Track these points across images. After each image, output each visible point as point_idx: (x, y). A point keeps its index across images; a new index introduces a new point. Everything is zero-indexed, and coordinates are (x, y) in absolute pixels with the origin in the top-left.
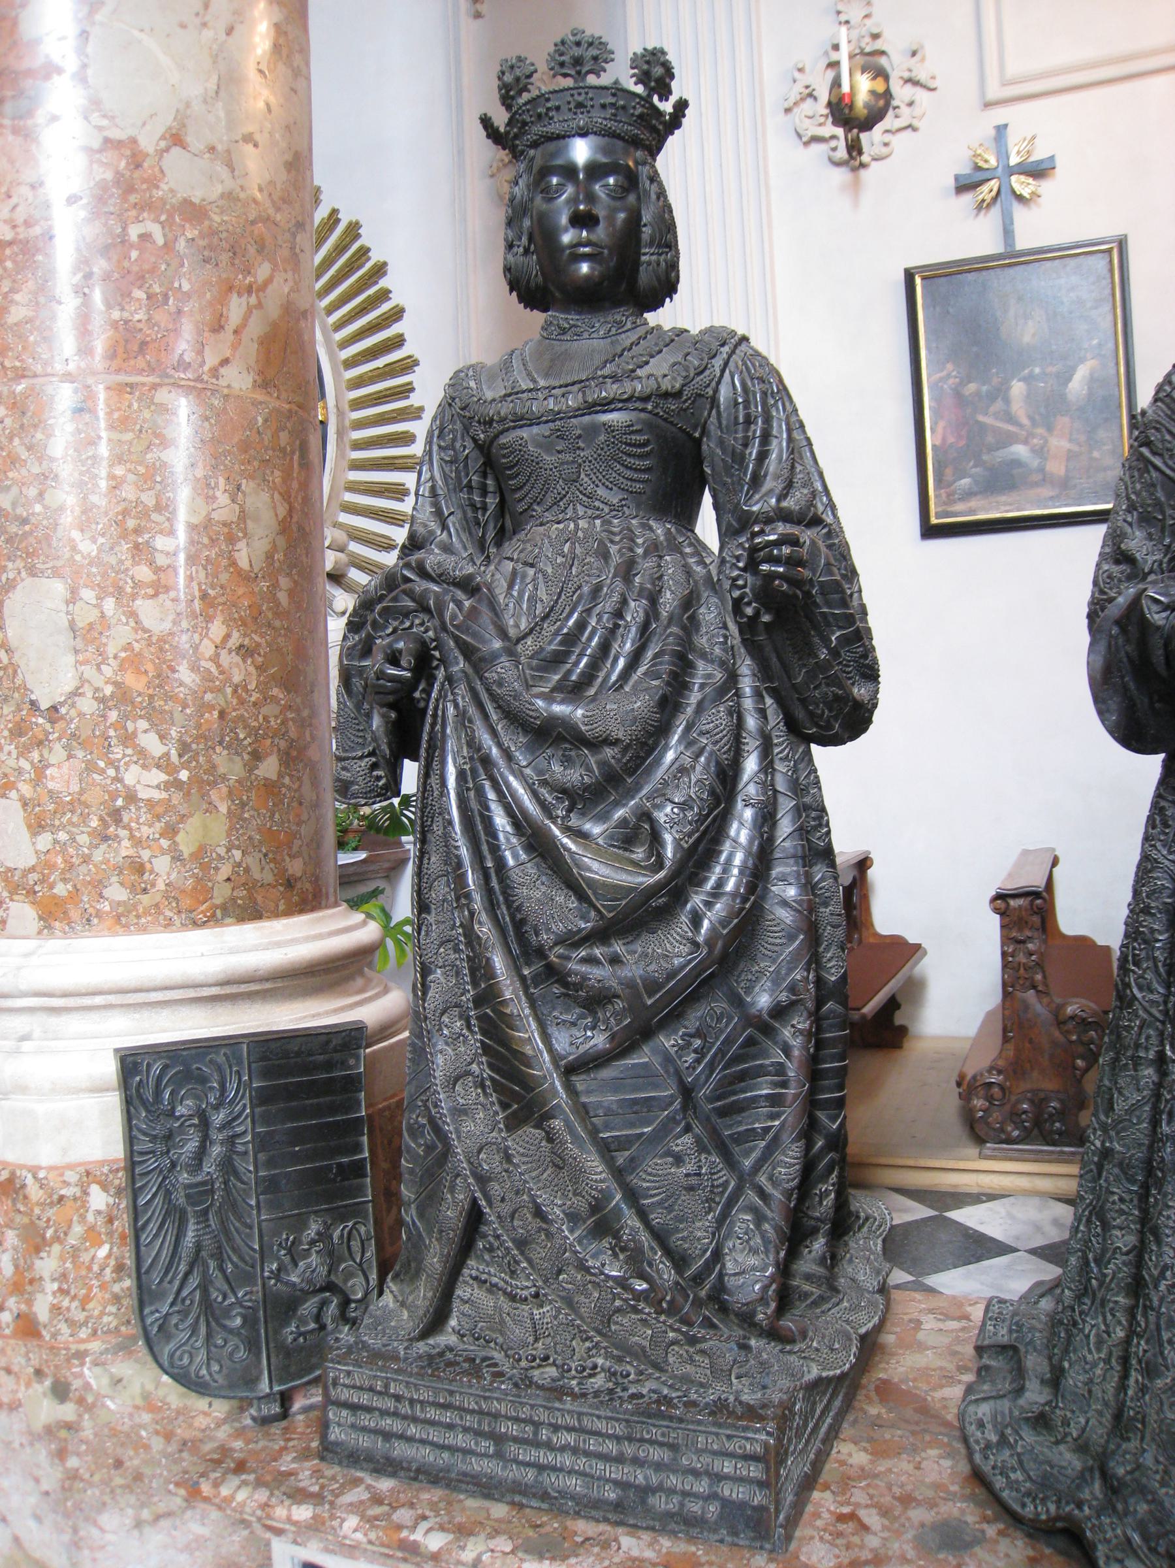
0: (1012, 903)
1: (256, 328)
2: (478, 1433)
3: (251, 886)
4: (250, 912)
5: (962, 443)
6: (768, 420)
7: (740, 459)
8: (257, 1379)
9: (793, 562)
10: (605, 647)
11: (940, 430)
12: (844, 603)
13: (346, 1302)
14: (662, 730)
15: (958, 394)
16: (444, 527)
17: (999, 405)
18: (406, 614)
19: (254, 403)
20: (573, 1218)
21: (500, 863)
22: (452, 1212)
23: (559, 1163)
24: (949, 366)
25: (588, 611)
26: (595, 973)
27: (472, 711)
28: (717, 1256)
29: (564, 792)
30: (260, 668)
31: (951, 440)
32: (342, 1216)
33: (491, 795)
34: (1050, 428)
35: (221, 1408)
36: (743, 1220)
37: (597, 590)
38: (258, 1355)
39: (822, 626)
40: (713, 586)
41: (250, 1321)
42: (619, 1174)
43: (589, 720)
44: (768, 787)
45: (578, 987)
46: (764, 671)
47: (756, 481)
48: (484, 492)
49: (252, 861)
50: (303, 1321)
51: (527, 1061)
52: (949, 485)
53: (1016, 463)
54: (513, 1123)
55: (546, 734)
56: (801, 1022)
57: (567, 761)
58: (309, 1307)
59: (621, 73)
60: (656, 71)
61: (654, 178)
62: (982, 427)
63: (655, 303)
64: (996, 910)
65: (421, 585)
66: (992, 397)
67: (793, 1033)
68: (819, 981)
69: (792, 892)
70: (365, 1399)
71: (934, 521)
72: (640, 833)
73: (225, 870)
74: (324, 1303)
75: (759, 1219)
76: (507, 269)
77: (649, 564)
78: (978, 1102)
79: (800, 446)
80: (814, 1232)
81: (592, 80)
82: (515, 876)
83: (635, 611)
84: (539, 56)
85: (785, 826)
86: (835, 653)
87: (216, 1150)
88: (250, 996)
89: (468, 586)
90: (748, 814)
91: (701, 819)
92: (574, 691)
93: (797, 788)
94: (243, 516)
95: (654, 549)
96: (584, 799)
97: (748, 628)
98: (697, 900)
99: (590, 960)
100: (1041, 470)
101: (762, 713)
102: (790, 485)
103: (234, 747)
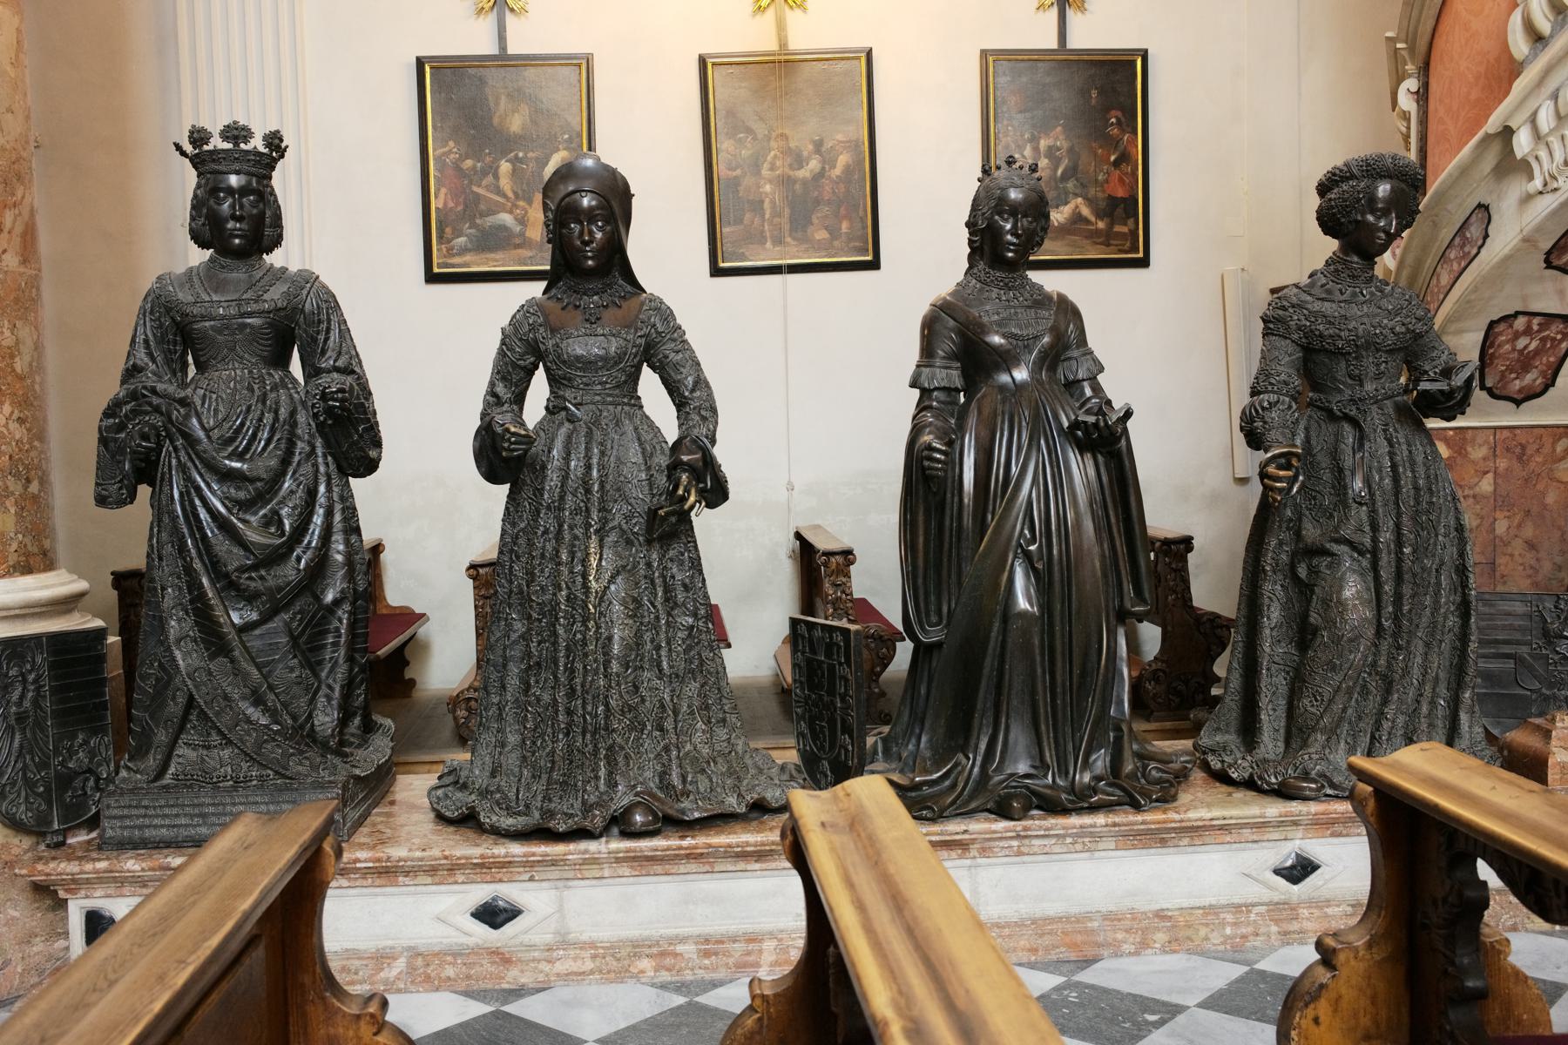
0: (481, 571)
1: (19, 229)
2: (192, 816)
3: (28, 555)
4: (27, 570)
5: (460, 208)
6: (329, 321)
7: (315, 340)
8: (52, 822)
9: (342, 401)
10: (254, 435)
11: (442, 196)
12: (365, 413)
13: (98, 779)
14: (284, 474)
15: (457, 167)
16: (153, 360)
17: (490, 178)
18: (147, 413)
19: (21, 274)
20: (244, 698)
21: (204, 537)
22: (174, 708)
23: (237, 672)
24: (451, 144)
25: (245, 418)
26: (253, 584)
27: (189, 464)
28: (310, 716)
29: (238, 502)
30: (29, 430)
31: (451, 204)
32: (95, 732)
33: (197, 502)
34: (530, 202)
35: (27, 842)
36: (321, 700)
37: (249, 408)
38: (51, 808)
39: (354, 423)
40: (303, 403)
41: (48, 790)
42: (265, 677)
43: (250, 470)
44: (330, 499)
45: (245, 590)
46: (327, 444)
47: (323, 352)
48: (175, 344)
49: (28, 540)
50: (75, 790)
51: (220, 625)
52: (449, 241)
53: (503, 228)
54: (212, 657)
55: (227, 476)
56: (347, 607)
57: (238, 488)
58: (78, 783)
59: (257, 143)
60: (275, 143)
61: (272, 193)
62: (478, 195)
63: (269, 250)
64: (470, 576)
65: (155, 401)
66: (484, 173)
67: (343, 614)
68: (355, 590)
69: (341, 547)
70: (126, 812)
71: (436, 270)
72: (274, 520)
73: (15, 546)
74: (87, 779)
75: (329, 698)
76: (191, 231)
77: (274, 395)
78: (462, 713)
79: (345, 333)
80: (355, 714)
81: (242, 146)
82: (213, 541)
83: (268, 418)
84: (215, 126)
85: (338, 517)
86: (361, 436)
87: (30, 694)
88: (33, 615)
89: (183, 402)
90: (321, 511)
91: (301, 514)
92: (240, 456)
93: (343, 499)
94: (17, 342)
95: (275, 388)
96: (246, 506)
97: (321, 427)
98: (298, 551)
99: (250, 578)
100: (522, 234)
101: (327, 464)
102: (340, 353)
103: (17, 476)
